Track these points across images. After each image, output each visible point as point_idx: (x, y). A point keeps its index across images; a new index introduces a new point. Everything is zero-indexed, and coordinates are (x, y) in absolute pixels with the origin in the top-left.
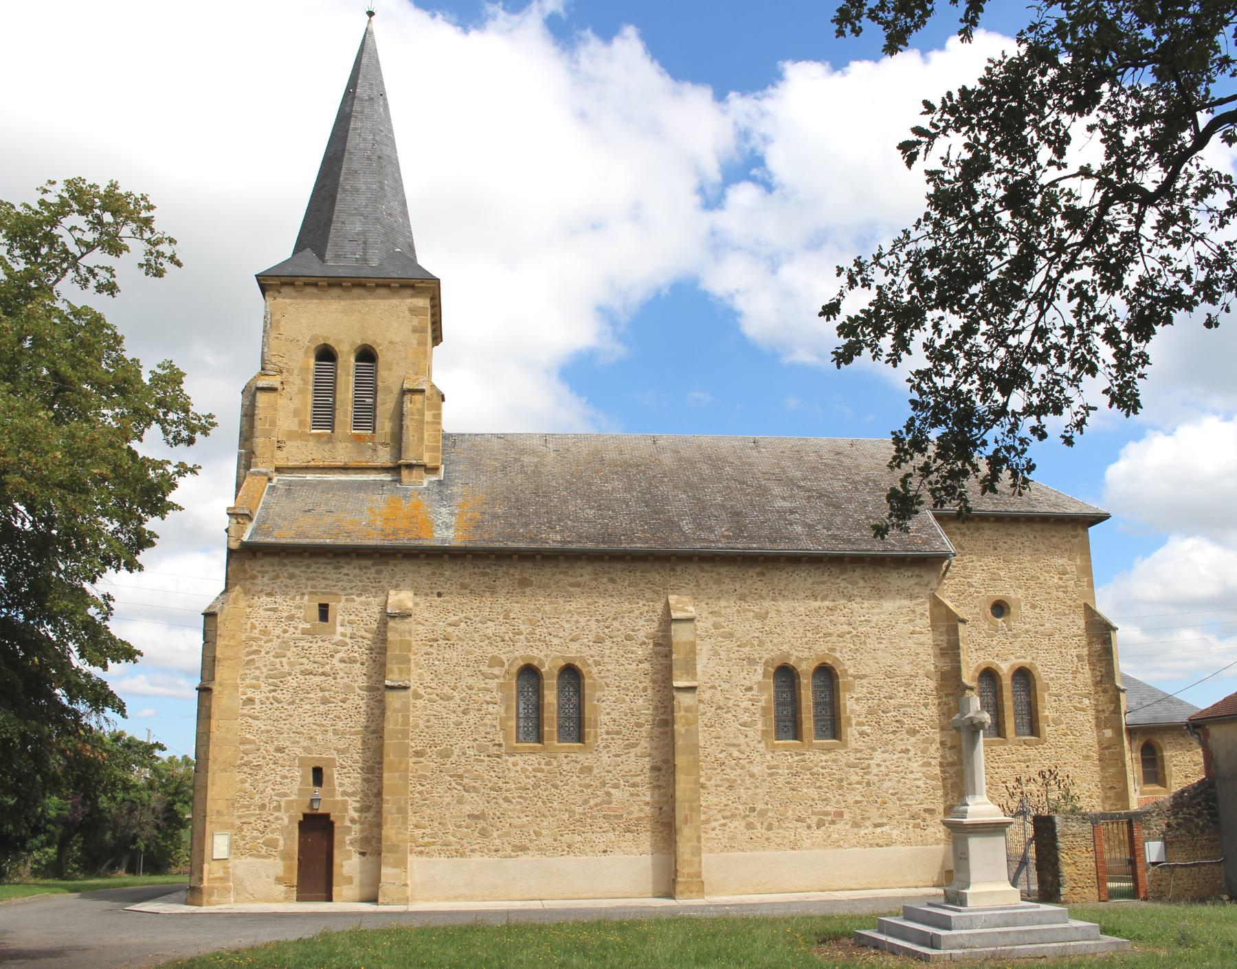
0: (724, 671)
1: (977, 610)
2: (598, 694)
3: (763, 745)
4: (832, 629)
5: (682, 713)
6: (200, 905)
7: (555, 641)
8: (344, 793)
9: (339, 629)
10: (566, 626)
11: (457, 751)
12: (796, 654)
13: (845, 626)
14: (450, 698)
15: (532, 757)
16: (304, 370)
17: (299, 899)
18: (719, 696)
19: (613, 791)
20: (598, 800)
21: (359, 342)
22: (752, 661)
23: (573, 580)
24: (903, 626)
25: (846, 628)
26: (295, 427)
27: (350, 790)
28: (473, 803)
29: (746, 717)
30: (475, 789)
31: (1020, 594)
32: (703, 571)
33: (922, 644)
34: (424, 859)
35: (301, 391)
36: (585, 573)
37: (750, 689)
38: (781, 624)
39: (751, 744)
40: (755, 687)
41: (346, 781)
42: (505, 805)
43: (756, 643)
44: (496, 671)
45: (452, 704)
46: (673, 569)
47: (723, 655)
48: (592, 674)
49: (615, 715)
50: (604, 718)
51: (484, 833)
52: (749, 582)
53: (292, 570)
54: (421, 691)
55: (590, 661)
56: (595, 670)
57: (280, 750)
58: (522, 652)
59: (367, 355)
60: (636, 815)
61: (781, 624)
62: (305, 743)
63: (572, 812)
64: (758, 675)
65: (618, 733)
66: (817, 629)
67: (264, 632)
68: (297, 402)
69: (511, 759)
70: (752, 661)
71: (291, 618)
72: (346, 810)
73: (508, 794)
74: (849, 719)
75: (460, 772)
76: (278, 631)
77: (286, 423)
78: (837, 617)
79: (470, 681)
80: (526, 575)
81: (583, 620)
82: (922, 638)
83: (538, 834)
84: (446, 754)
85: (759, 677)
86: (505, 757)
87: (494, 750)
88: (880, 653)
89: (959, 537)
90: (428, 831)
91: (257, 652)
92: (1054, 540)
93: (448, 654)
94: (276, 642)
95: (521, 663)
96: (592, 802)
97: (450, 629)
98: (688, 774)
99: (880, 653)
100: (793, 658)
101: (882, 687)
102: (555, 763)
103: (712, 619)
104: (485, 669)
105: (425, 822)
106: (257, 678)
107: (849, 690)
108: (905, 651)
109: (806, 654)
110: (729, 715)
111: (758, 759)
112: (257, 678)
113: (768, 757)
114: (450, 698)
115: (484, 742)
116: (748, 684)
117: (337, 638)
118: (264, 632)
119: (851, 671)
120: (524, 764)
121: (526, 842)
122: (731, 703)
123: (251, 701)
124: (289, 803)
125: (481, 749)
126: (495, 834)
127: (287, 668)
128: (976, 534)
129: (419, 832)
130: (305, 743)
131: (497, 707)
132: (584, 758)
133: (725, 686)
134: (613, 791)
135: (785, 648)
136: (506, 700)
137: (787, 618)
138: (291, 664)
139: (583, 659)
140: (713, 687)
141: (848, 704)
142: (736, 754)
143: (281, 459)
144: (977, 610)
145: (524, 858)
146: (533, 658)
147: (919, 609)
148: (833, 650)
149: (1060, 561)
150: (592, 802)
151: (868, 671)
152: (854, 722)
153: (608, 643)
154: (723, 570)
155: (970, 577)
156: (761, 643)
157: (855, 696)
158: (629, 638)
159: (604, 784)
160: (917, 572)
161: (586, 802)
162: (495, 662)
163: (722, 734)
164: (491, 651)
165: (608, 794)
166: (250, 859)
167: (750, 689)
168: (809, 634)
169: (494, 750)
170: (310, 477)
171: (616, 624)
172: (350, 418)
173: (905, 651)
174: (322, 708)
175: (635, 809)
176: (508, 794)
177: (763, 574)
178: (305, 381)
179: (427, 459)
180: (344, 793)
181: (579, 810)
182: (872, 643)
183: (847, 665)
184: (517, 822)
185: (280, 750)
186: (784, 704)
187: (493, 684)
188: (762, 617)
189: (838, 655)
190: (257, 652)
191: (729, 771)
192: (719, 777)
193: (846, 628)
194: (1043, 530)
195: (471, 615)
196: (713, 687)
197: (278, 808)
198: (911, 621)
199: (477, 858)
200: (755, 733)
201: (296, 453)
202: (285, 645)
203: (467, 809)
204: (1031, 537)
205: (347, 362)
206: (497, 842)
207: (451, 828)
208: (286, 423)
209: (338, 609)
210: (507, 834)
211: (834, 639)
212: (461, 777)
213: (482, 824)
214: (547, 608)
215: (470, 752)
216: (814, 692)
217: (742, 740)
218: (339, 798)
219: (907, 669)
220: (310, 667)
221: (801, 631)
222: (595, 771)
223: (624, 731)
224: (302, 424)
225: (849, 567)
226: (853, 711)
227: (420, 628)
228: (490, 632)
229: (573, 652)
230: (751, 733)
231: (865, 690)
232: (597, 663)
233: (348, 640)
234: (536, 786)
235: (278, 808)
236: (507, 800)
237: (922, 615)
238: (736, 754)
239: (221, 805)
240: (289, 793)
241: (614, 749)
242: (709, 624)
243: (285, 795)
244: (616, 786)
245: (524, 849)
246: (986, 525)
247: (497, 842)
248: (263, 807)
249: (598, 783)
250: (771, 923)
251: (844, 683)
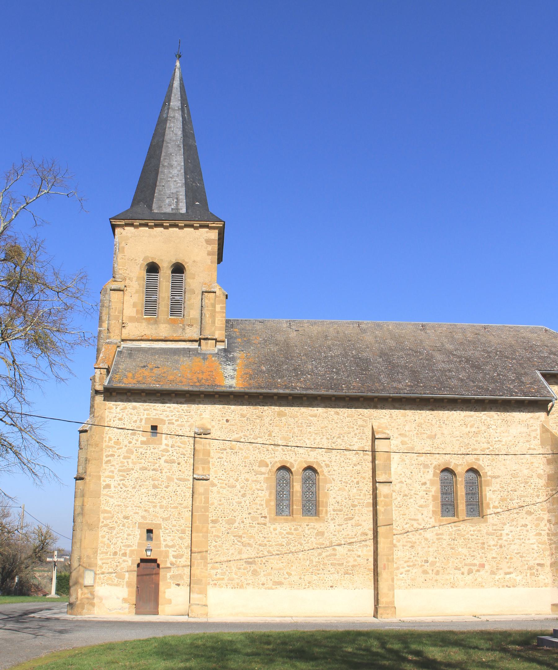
0: (408, 472)
2: (328, 486)
3: (433, 520)
5: (382, 498)
13: (485, 444)
17: (137, 613)
20: (328, 553)
21: (174, 261)
25: (486, 446)
29: (422, 502)
39: (426, 519)
40: (428, 482)
41: (168, 538)
44: (263, 469)
47: (407, 461)
49: (339, 499)
50: (331, 501)
54: (216, 481)
55: (323, 465)
56: (326, 470)
57: (126, 518)
58: (280, 457)
63: (311, 561)
65: (341, 510)
70: (426, 466)
72: (167, 557)
74: (488, 504)
75: (241, 533)
76: (126, 442)
83: (289, 574)
84: (231, 522)
87: (262, 520)
90: (219, 571)
91: (112, 455)
94: (124, 449)
102: (300, 529)
103: (400, 439)
104: (256, 468)
106: (113, 472)
107: (488, 485)
112: (113, 472)
116: (423, 480)
120: (281, 529)
122: (413, 492)
124: (132, 552)
126: (262, 574)
127: (131, 466)
131: (264, 493)
132: (319, 526)
133: (409, 481)
138: (134, 463)
139: (317, 463)
140: (401, 482)
141: (488, 494)
143: (126, 333)
146: (287, 462)
152: (491, 506)
162: (263, 464)
165: (334, 550)
167: (425, 484)
169: (262, 520)
170: (144, 345)
171: (339, 441)
174: (153, 491)
180: (167, 546)
185: (126, 518)
187: (261, 478)
190: (112, 455)
198: (528, 441)
205: (165, 274)
208: (130, 311)
210: (269, 574)
212: (240, 537)
213: (254, 567)
214: (296, 430)
218: (163, 548)
219: (526, 472)
222: (326, 534)
226: (491, 499)
232: (327, 466)
233: (170, 449)
235: (125, 554)
237: (535, 437)
240: (133, 545)
243: (129, 546)
245: (280, 583)
248: (115, 554)
251: (485, 481)
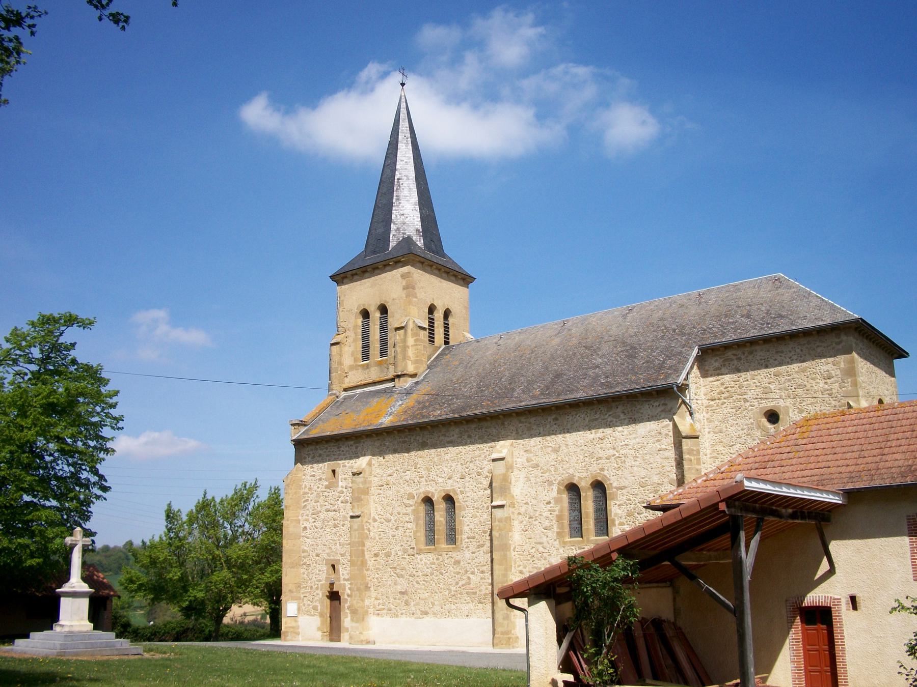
0: (533, 493)
1: (752, 420)
2: (463, 513)
3: (557, 542)
4: (602, 454)
5: (497, 523)
6: (513, 647)
7: (440, 480)
8: (345, 580)
9: (340, 484)
10: (446, 469)
11: (393, 553)
12: (577, 474)
13: (611, 451)
14: (390, 521)
15: (429, 555)
16: (356, 326)
17: (331, 640)
18: (530, 510)
19: (471, 576)
20: (463, 582)
21: (379, 304)
22: (551, 483)
23: (448, 439)
24: (652, 446)
25: (612, 452)
26: (352, 363)
27: (347, 577)
28: (403, 585)
29: (547, 523)
30: (402, 576)
31: (789, 402)
32: (520, 422)
33: (667, 458)
34: (379, 618)
35: (355, 340)
36: (455, 432)
37: (549, 503)
38: (568, 454)
39: (550, 542)
40: (552, 501)
41: (345, 572)
42: (417, 586)
43: (552, 470)
44: (411, 502)
45: (390, 524)
46: (503, 424)
47: (533, 479)
48: (459, 499)
49: (472, 526)
50: (466, 528)
51: (407, 603)
52: (548, 426)
53: (320, 452)
54: (376, 517)
55: (458, 492)
56: (460, 497)
57: (318, 555)
58: (422, 490)
59: (383, 310)
60: (483, 592)
61: (568, 454)
62: (328, 551)
63: (450, 590)
64: (554, 493)
65: (474, 538)
66: (592, 455)
67: (310, 489)
68: (351, 349)
69: (419, 557)
70: (551, 483)
71: (320, 479)
72: (344, 589)
73: (418, 579)
74: (614, 520)
75: (395, 565)
76: (315, 488)
77: (348, 361)
78: (606, 444)
79: (399, 509)
80: (425, 439)
81: (454, 465)
82: (667, 454)
83: (433, 604)
84: (388, 555)
85: (554, 494)
86: (416, 556)
87: (411, 551)
88: (635, 468)
89: (735, 362)
90: (381, 601)
91: (307, 500)
92: (819, 350)
93: (389, 493)
94: (315, 493)
95: (423, 496)
96: (460, 584)
97: (389, 478)
98: (500, 565)
99: (635, 468)
100: (576, 478)
101: (637, 495)
102: (441, 559)
103: (526, 455)
104: (405, 501)
105: (379, 596)
106: (307, 515)
107: (613, 499)
108: (654, 465)
109: (585, 474)
110: (537, 522)
111: (555, 553)
112: (307, 515)
113: (561, 551)
114: (390, 521)
115: (406, 546)
116: (548, 499)
117: (340, 489)
118: (310, 489)
119: (615, 485)
120: (426, 560)
121: (427, 609)
122: (538, 513)
123: (305, 528)
124: (322, 585)
125: (405, 551)
126: (412, 604)
127: (319, 509)
128: (750, 357)
129: (377, 602)
130: (328, 551)
131: (411, 525)
132: (456, 555)
133: (534, 502)
134: (471, 576)
135: (571, 471)
136: (417, 519)
137: (572, 449)
138: (321, 506)
139: (454, 490)
140: (527, 503)
141: (613, 509)
142: (541, 549)
143: (348, 383)
144: (752, 420)
145: (428, 619)
146: (429, 492)
147: (664, 431)
148: (602, 470)
149: (825, 368)
150: (460, 584)
151: (626, 483)
152: (617, 522)
153: (467, 479)
154: (532, 420)
155: (745, 394)
156: (556, 470)
157: (618, 503)
158: (479, 474)
159: (466, 572)
160: (663, 402)
161: (457, 583)
162: (411, 496)
163: (533, 536)
164: (409, 490)
165: (469, 578)
166: (308, 617)
167: (549, 503)
168: (587, 459)
169: (411, 551)
170: (359, 391)
171: (471, 465)
172: (378, 352)
173: (654, 465)
174: (334, 530)
175: (483, 588)
176: (418, 579)
177: (556, 419)
178: (356, 334)
179: (411, 369)
180: (345, 580)
181: (453, 588)
182: (630, 461)
183: (613, 482)
184: (422, 596)
185: (318, 555)
186: (573, 511)
187: (409, 510)
188: (556, 451)
189: (605, 473)
190: (307, 500)
191: (536, 561)
192: (531, 566)
193: (612, 452)
194: (809, 343)
195: (398, 468)
196: (527, 503)
197: (317, 588)
198: (659, 441)
199: (403, 619)
200: (552, 534)
201: (355, 378)
202: (318, 496)
203: (399, 588)
204: (798, 351)
205: (376, 315)
206: (413, 609)
207: (392, 600)
208: (348, 361)
209: (339, 471)
210: (417, 604)
211: (603, 461)
212: (395, 568)
213: (406, 597)
214: (436, 459)
215: (400, 553)
216: (595, 501)
217: (544, 539)
218: (342, 582)
219: (656, 479)
220: (329, 507)
221: (582, 457)
222: (462, 563)
223: (477, 536)
224: (356, 360)
225: (614, 405)
226: (616, 514)
227: (376, 479)
228: (407, 478)
229: (449, 486)
230: (550, 534)
231: (625, 498)
232: (462, 492)
233: (344, 490)
234: (432, 574)
235: (317, 588)
236: (418, 583)
237: (667, 435)
238: (541, 549)
239: (291, 587)
241: (472, 548)
242: (524, 460)
243: (320, 581)
244: (473, 573)
245: (426, 613)
246: (757, 348)
247: (413, 609)
248: (311, 587)
249: (462, 571)
250: (247, 653)
251: (610, 493)
